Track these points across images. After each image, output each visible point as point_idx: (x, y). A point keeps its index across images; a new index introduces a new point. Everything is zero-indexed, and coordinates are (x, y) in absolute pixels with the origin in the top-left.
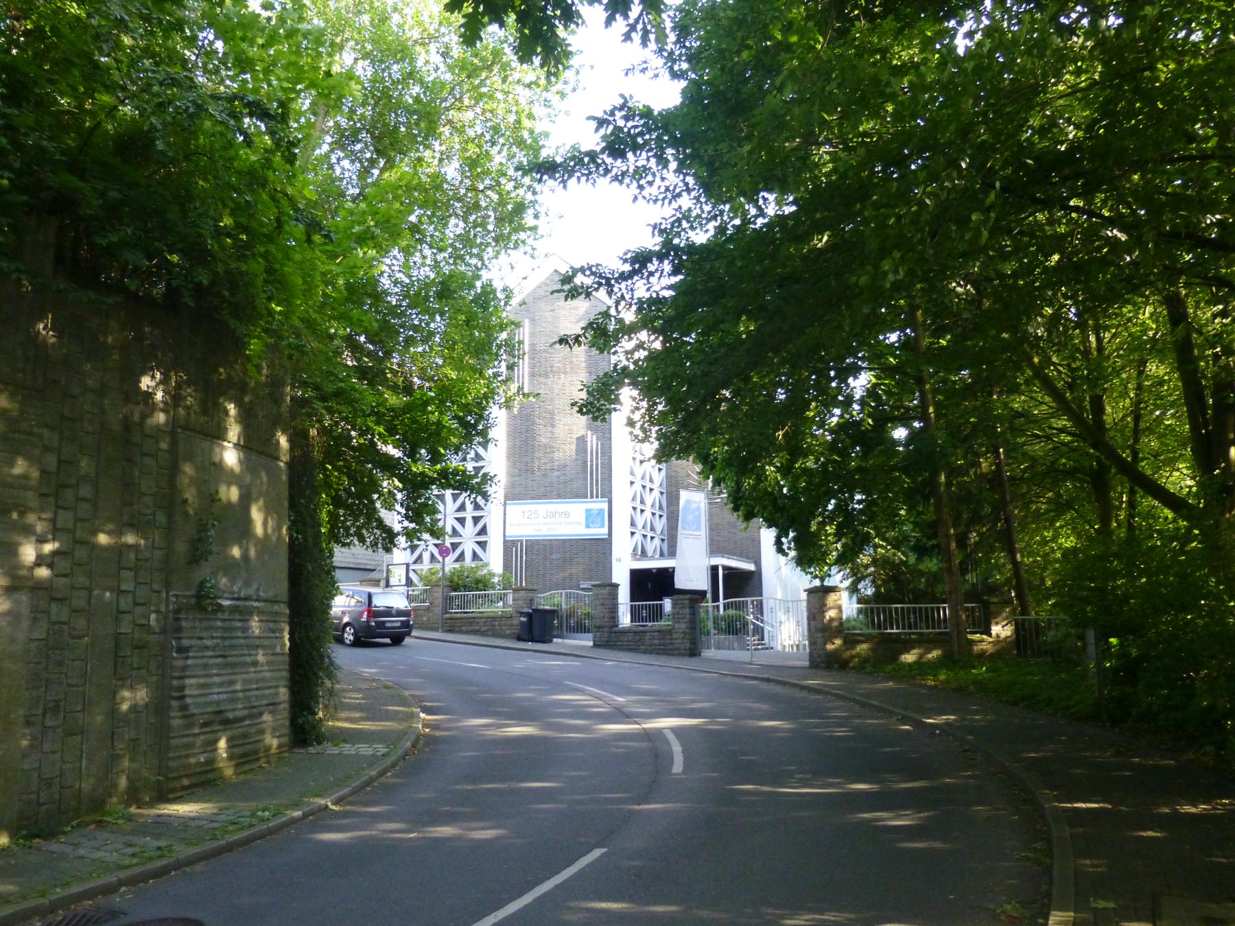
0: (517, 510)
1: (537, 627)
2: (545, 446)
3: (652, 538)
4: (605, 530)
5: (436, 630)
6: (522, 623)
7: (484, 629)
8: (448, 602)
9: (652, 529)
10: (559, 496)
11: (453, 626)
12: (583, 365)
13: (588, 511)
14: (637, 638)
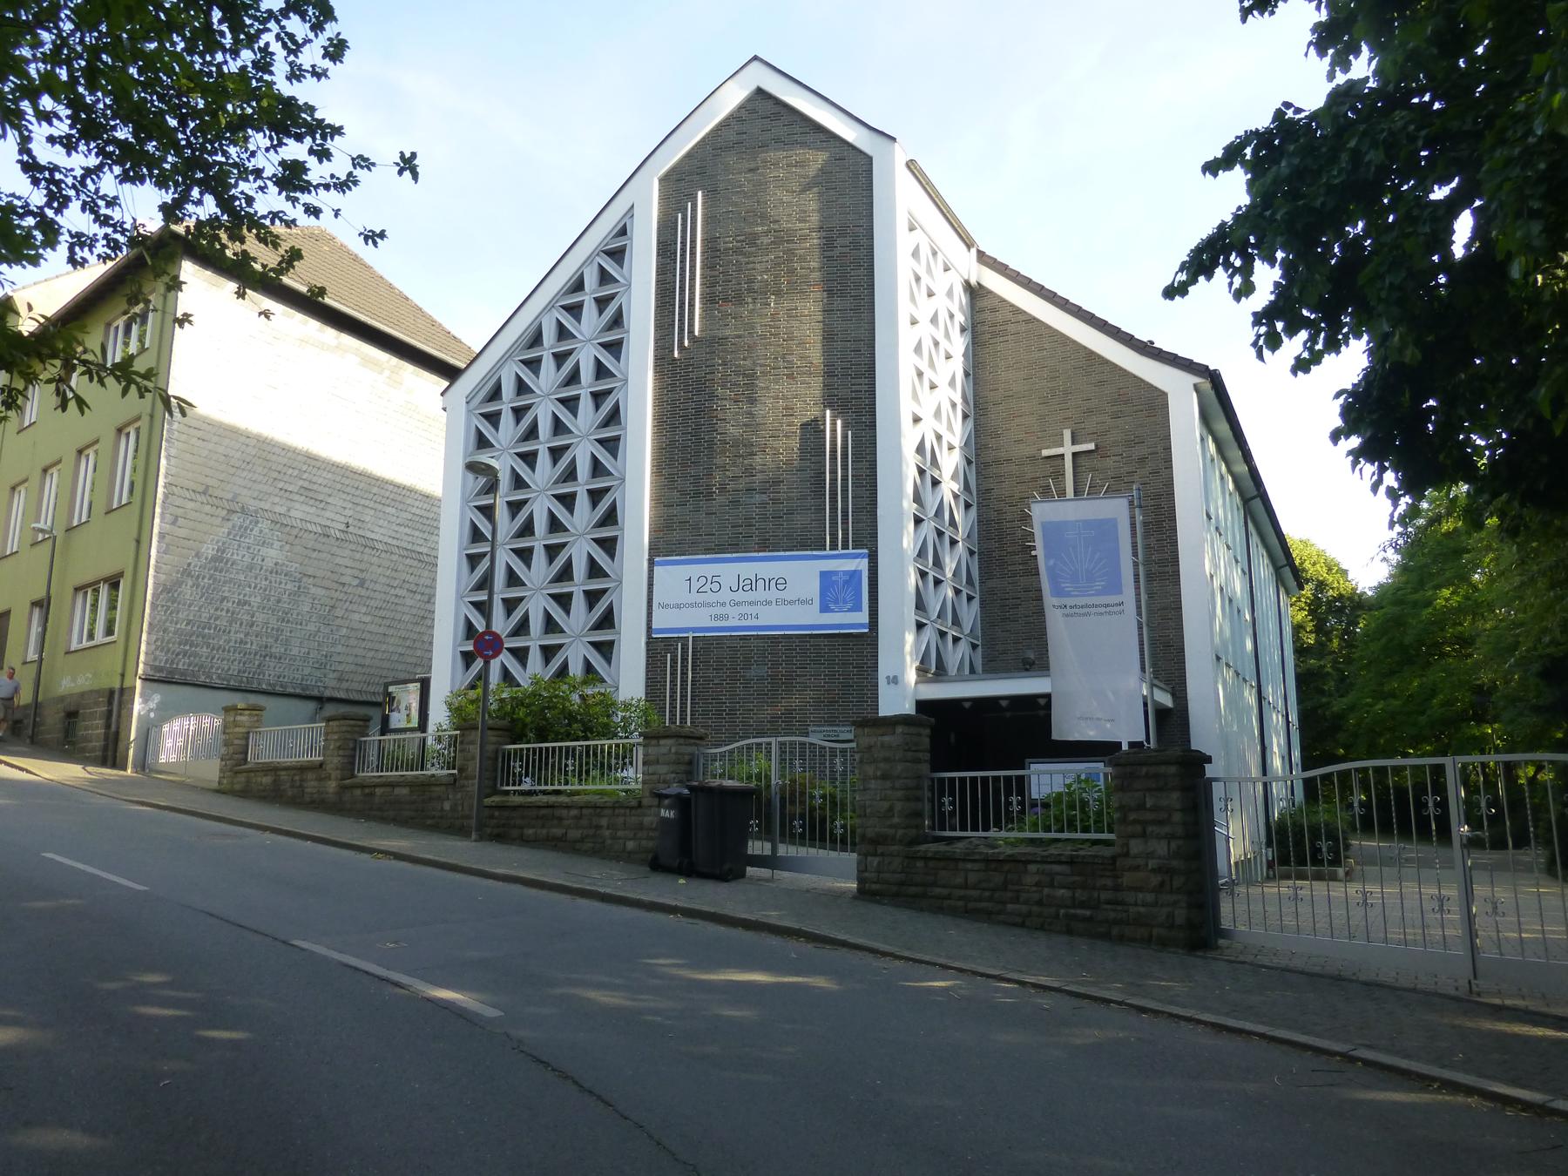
0: (675, 577)
1: (706, 834)
3: (956, 640)
4: (863, 617)
5: (461, 831)
6: (664, 820)
7: (574, 834)
8: (497, 769)
9: (956, 622)
10: (764, 545)
11: (502, 826)
12: (816, 275)
13: (825, 576)
14: (998, 879)
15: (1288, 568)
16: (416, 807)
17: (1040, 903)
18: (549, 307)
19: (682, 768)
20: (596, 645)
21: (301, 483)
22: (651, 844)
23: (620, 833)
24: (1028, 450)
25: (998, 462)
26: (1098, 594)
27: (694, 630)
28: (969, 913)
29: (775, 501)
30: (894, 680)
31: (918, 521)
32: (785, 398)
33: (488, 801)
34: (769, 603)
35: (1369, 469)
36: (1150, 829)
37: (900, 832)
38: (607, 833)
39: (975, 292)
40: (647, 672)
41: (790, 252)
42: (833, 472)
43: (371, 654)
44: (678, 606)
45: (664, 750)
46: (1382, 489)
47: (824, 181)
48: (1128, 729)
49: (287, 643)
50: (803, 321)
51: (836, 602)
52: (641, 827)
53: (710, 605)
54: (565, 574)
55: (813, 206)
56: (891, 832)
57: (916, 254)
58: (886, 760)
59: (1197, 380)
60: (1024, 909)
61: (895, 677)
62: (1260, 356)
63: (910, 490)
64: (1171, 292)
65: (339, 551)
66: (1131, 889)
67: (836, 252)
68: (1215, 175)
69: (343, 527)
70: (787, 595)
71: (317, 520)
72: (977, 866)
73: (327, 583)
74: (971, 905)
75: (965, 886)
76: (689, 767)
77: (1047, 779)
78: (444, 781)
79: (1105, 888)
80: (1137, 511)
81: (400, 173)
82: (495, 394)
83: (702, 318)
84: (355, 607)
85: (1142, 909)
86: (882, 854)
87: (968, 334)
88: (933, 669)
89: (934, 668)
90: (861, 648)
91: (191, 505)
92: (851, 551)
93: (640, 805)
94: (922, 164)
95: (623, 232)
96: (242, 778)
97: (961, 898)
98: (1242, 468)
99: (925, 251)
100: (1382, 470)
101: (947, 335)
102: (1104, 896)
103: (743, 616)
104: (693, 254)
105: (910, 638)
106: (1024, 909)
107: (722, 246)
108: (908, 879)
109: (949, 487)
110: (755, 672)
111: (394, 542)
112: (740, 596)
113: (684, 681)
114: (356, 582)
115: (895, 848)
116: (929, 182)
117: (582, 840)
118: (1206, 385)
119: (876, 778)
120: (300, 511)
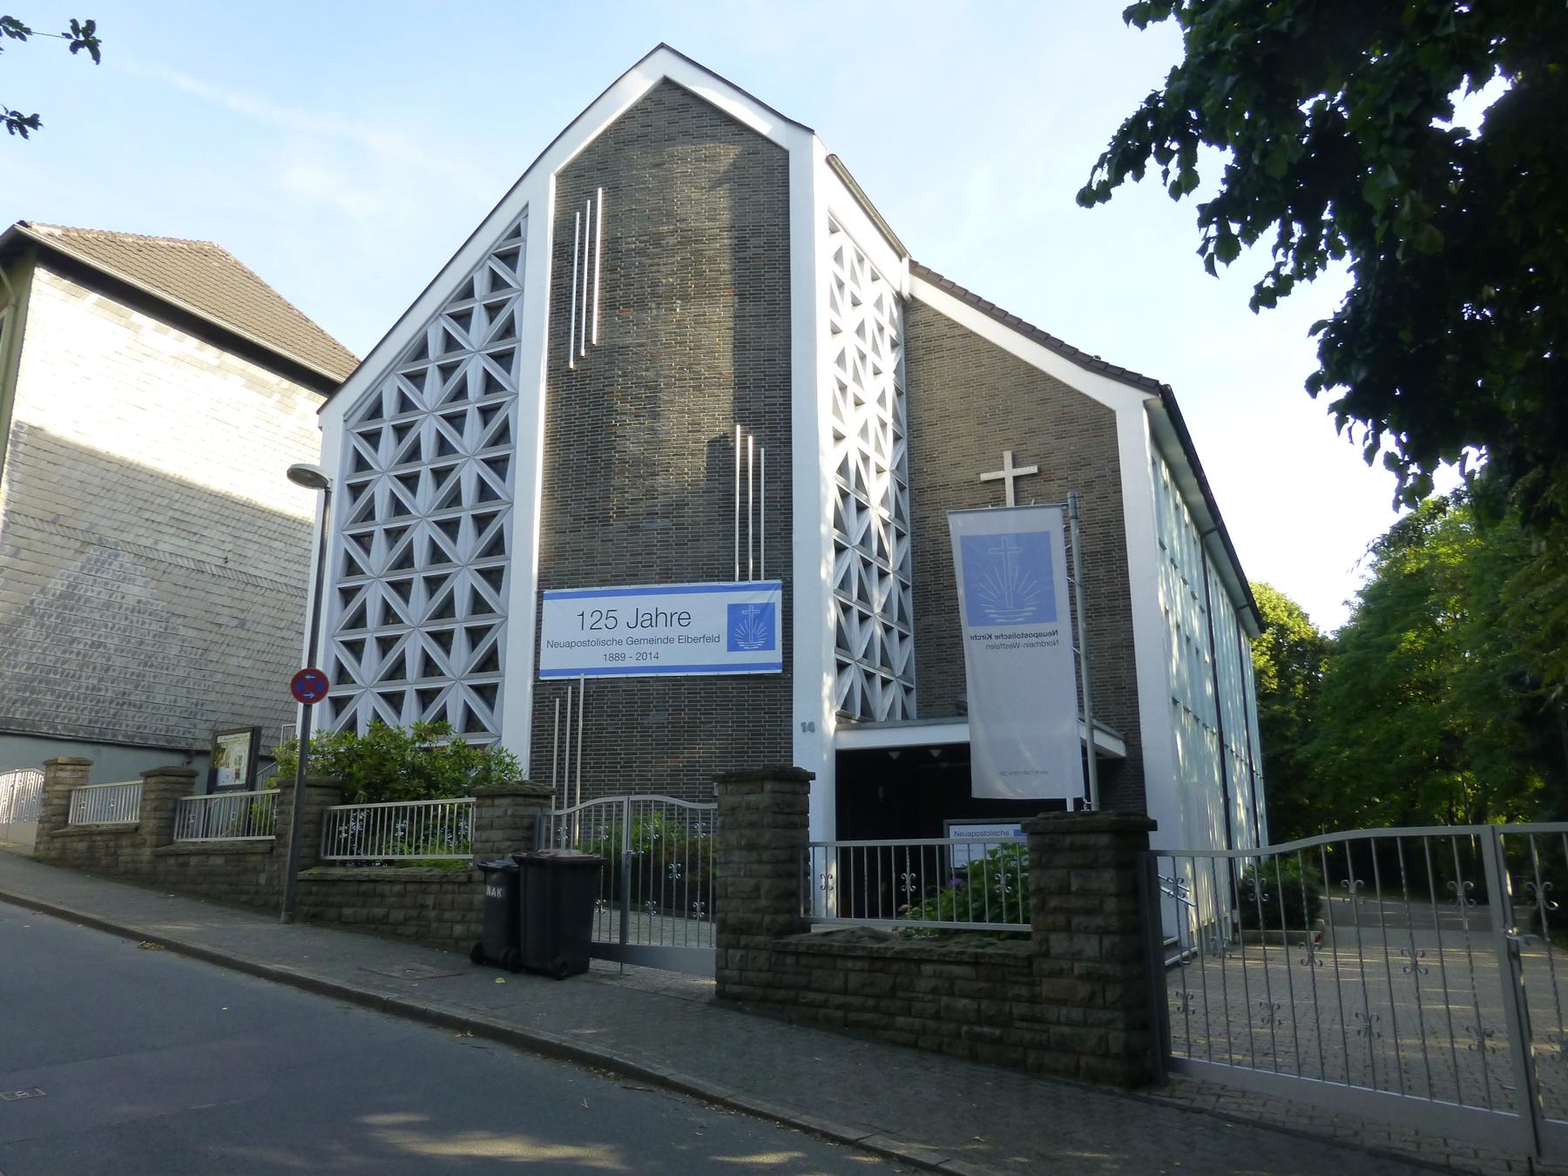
0: (565, 611)
2: (636, 463)
3: (885, 683)
4: (776, 656)
6: (490, 901)
8: (317, 834)
9: (885, 662)
10: (666, 576)
11: (317, 905)
12: (727, 278)
13: (733, 609)
15: (1247, 608)
16: (224, 883)
17: (937, 1016)
18: (435, 316)
19: (521, 833)
20: (478, 689)
21: (171, 513)
22: (480, 928)
23: (447, 915)
24: (965, 474)
25: (933, 488)
26: (1028, 621)
27: (587, 671)
28: (850, 1027)
29: (679, 526)
30: (810, 728)
31: (840, 549)
32: (690, 412)
33: (303, 874)
34: (670, 640)
35: (1360, 428)
36: (1076, 920)
37: (768, 918)
38: (433, 914)
39: (907, 305)
40: (534, 719)
41: (699, 253)
42: (744, 493)
43: (251, 702)
44: (569, 645)
45: (499, 812)
46: (1379, 457)
47: (735, 177)
48: (1065, 782)
49: (149, 690)
50: (711, 329)
51: (746, 639)
52: (470, 907)
53: (604, 643)
54: (446, 609)
55: (724, 203)
56: (757, 917)
57: (838, 257)
58: (752, 825)
59: (1147, 396)
60: (917, 1023)
61: (811, 724)
62: (1210, 268)
63: (829, 514)
64: (1090, 197)
65: (214, 589)
66: (1050, 1001)
67: (749, 253)
68: (1143, 26)
69: (220, 562)
70: (692, 631)
71: (191, 554)
72: (859, 965)
73: (198, 624)
74: (852, 1016)
75: (845, 991)
76: (530, 832)
77: (968, 844)
78: (261, 848)
79: (1017, 999)
80: (1073, 523)
81: (75, 47)
82: (376, 412)
83: (600, 324)
84: (232, 650)
85: (1066, 1030)
86: (746, 947)
87: (900, 352)
88: (858, 715)
89: (856, 713)
90: (772, 693)
91: (37, 535)
92: (762, 581)
93: (470, 880)
94: (844, 159)
95: (517, 233)
96: (58, 844)
97: (839, 1007)
98: (1198, 498)
99: (849, 256)
100: (1378, 429)
101: (875, 348)
102: (1020, 1009)
103: (641, 656)
104: (592, 256)
105: (828, 680)
106: (917, 1023)
107: (624, 247)
108: (777, 977)
109: (878, 513)
110: (654, 718)
111: (282, 580)
112: (639, 633)
113: (574, 729)
114: (235, 623)
115: (762, 939)
116: (852, 181)
117: (404, 922)
118: (1157, 402)
119: (739, 848)
120: (168, 544)
